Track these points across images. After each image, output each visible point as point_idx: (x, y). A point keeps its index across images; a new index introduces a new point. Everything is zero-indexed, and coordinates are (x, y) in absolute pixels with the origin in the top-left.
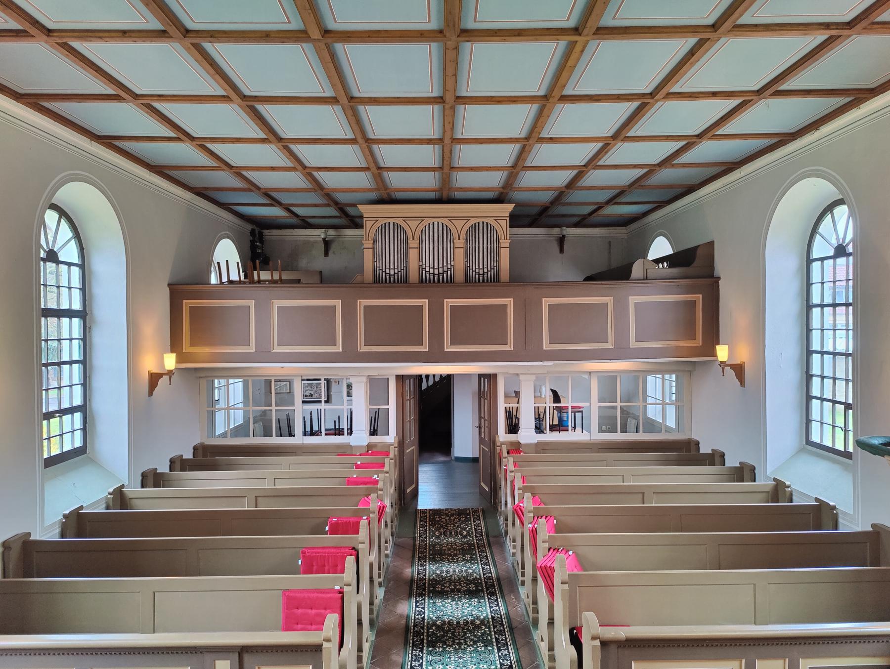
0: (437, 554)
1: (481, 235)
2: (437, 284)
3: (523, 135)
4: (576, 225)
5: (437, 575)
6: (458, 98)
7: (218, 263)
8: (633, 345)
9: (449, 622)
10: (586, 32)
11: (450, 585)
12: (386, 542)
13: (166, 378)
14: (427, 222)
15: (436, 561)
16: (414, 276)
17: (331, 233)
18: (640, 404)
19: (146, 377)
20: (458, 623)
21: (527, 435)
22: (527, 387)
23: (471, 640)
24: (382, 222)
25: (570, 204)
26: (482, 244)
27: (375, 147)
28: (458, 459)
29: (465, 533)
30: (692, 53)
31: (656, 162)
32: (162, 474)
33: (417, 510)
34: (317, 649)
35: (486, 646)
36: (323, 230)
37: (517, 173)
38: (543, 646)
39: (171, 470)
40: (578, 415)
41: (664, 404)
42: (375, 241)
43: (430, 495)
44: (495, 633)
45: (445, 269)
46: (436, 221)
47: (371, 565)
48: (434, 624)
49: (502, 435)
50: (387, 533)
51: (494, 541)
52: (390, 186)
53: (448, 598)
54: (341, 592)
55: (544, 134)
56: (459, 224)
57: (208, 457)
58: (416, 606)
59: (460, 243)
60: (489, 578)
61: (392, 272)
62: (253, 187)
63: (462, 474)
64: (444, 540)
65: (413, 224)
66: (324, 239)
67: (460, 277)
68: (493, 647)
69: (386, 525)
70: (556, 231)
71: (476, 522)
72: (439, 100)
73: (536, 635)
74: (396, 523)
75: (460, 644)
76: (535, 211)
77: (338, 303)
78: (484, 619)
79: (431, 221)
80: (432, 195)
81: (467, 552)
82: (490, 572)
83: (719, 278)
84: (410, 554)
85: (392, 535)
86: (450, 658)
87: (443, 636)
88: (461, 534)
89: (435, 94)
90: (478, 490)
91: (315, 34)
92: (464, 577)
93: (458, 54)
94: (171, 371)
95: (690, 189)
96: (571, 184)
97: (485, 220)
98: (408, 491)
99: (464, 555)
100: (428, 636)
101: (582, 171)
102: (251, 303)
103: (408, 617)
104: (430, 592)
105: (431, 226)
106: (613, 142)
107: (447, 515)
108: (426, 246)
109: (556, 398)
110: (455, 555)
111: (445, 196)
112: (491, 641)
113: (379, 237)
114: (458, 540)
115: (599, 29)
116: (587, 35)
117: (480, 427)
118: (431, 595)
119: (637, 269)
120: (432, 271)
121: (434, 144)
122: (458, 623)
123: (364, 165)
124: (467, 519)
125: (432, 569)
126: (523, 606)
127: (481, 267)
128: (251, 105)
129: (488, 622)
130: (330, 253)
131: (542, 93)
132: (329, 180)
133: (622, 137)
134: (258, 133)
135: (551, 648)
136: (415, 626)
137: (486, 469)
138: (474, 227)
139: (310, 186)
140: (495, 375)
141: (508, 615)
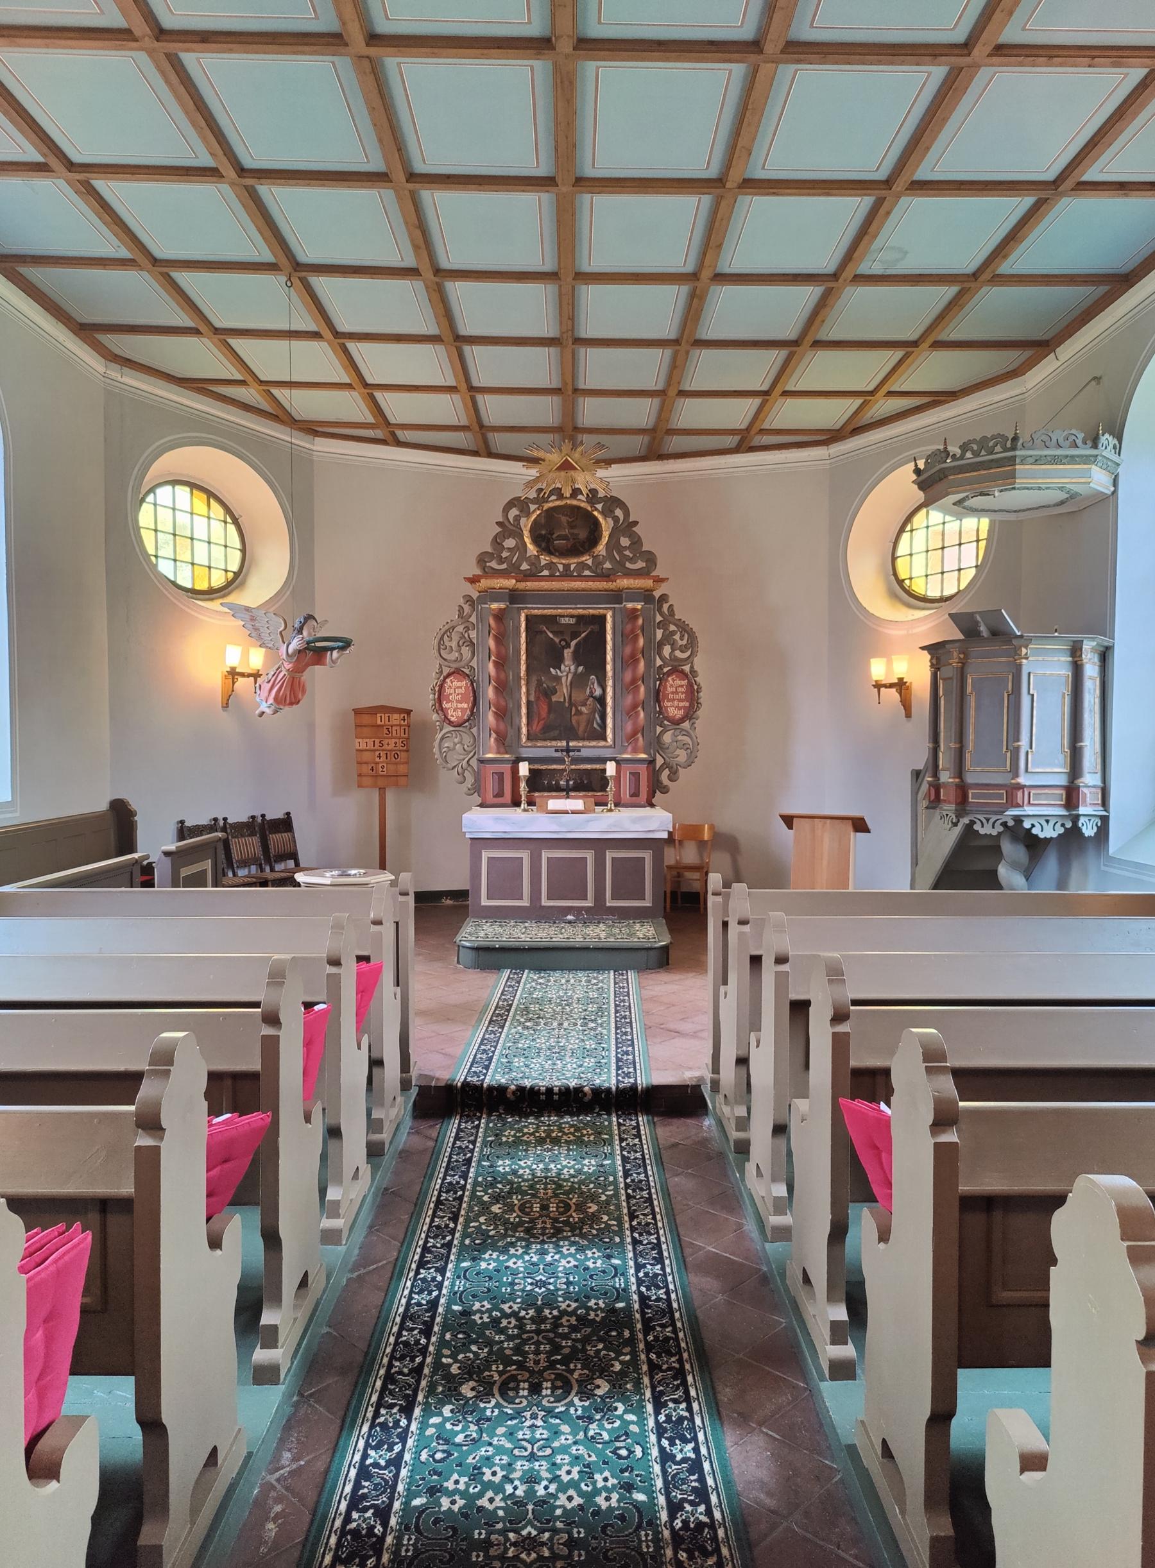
20: (535, 1389)
23: (502, 1331)
35: (466, 1313)
68: (448, 1309)
75: (539, 1319)
86: (568, 1283)
100: (632, 1342)
103: (716, 1410)
141: (347, 1424)
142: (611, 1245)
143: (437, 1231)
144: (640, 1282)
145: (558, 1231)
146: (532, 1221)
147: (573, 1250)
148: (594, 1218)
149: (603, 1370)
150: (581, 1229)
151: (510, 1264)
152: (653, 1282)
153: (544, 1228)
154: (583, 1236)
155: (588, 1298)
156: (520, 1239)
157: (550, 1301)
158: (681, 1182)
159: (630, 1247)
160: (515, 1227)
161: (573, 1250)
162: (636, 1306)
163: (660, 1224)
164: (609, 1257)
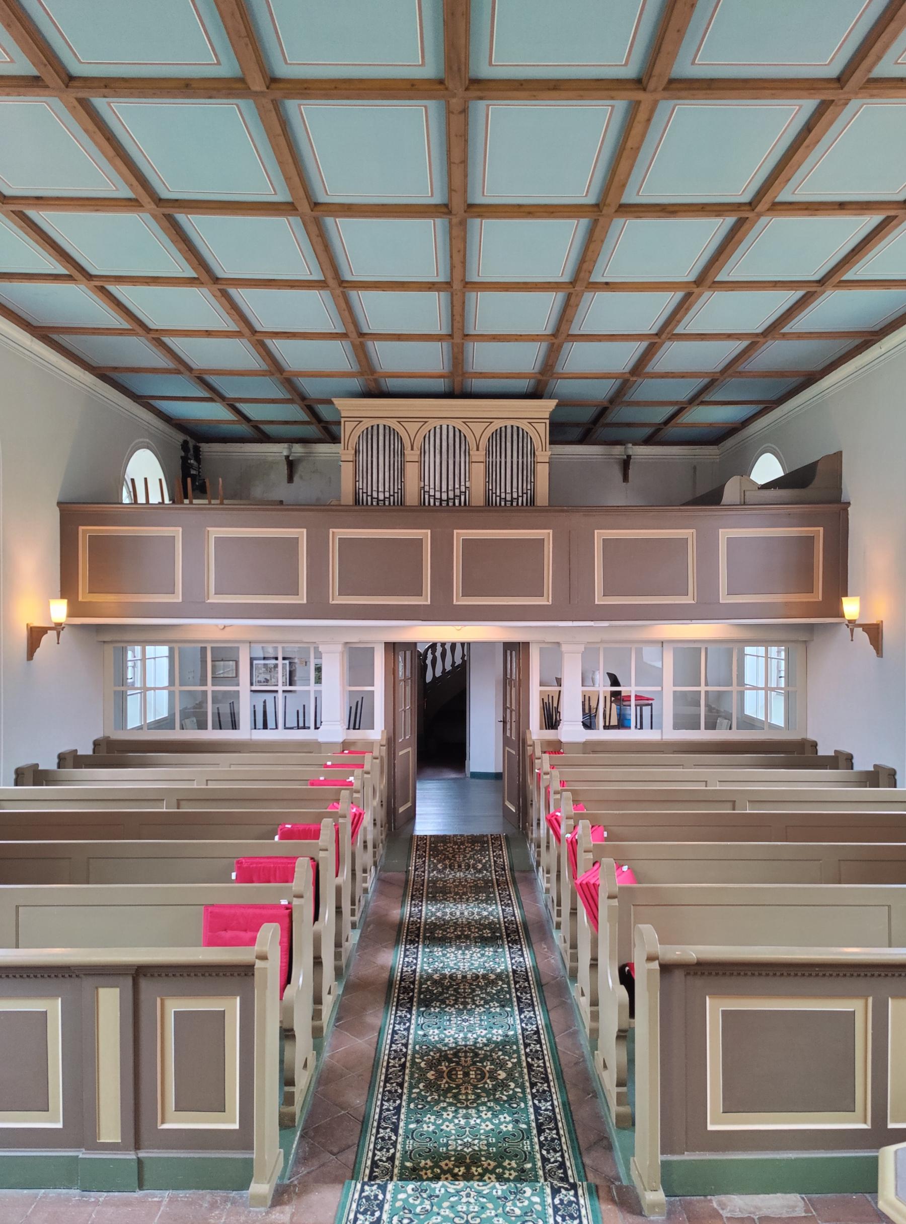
0: (439, 892)
1: (509, 445)
2: (446, 511)
3: (566, 278)
4: (648, 441)
5: (438, 918)
6: (470, 206)
7: (133, 480)
8: (724, 598)
9: (451, 977)
10: (652, 85)
11: (455, 930)
12: (365, 871)
13: (52, 634)
14: (432, 424)
15: (436, 900)
16: (412, 498)
17: (298, 449)
18: (734, 688)
19: (24, 634)
20: (464, 977)
21: (571, 730)
22: (571, 664)
23: (482, 999)
24: (367, 423)
25: (638, 404)
26: (511, 457)
27: (353, 294)
28: (475, 775)
29: (480, 866)
30: (808, 128)
31: (760, 331)
32: (46, 772)
33: (412, 837)
34: (246, 971)
36: (286, 445)
37: (560, 347)
38: (584, 1002)
39: (59, 767)
40: (646, 710)
41: (767, 689)
42: (357, 452)
43: (432, 816)
44: (517, 990)
45: (457, 492)
46: (444, 423)
47: (339, 890)
48: (430, 977)
49: (536, 732)
50: (366, 858)
51: (522, 875)
52: (378, 369)
53: (451, 946)
54: (289, 908)
55: (596, 277)
56: (478, 428)
57: (112, 753)
58: (405, 956)
59: (479, 455)
60: (511, 922)
61: (381, 497)
62: (182, 366)
63: (482, 795)
64: (450, 875)
65: (412, 427)
66: (287, 457)
67: (478, 497)
68: (512, 1007)
69: (365, 847)
70: (618, 450)
71: (497, 855)
72: (443, 210)
73: (574, 990)
74: (381, 850)
75: (465, 1004)
76: (587, 415)
77: (301, 534)
78: (502, 973)
79: (437, 423)
80: (440, 385)
81: (481, 890)
82: (514, 915)
83: (849, 503)
84: (401, 891)
85: (375, 864)
86: (450, 1020)
87: (441, 994)
88: (474, 868)
89: (437, 199)
90: (501, 814)
91: (257, 85)
92: (476, 921)
93: (466, 124)
94: (61, 624)
95: (810, 379)
96: (639, 368)
97: (516, 423)
98: (401, 810)
99: (477, 893)
100: (420, 993)
101: (654, 343)
102: (177, 532)
103: (392, 969)
104: (425, 938)
105: (438, 430)
106: (696, 290)
107: (455, 843)
108: (430, 459)
109: (615, 682)
110: (465, 894)
111: (457, 390)
112: (511, 999)
113: (363, 447)
114: (470, 875)
115: (671, 81)
116: (655, 90)
117: (504, 722)
118: (427, 942)
119: (731, 491)
120: (438, 495)
121: (438, 290)
122: (464, 977)
123: (340, 329)
124: (483, 849)
125: (430, 911)
126: (558, 958)
127: (509, 490)
128: (169, 213)
129: (507, 976)
130: (296, 478)
131: (591, 200)
132: (292, 355)
133: (708, 282)
134: (182, 268)
135: (594, 1003)
136: (402, 980)
137: (515, 783)
138: (499, 434)
139: (265, 367)
140: (527, 645)
141: (535, 968)
142: (421, 1044)
143: (537, 1055)
144: (409, 1020)
145: (456, 1055)
146: (474, 1063)
147: (447, 1040)
148: (431, 1065)
149: (435, 982)
150: (440, 1056)
151: (485, 1032)
152: (402, 1020)
153: (466, 1057)
154: (440, 1050)
155: (439, 1012)
156: (481, 1049)
157: (460, 1012)
158: (356, 1100)
159: (410, 1041)
160: (485, 1058)
161: (447, 1040)
162: (414, 1008)
163: (386, 1058)
164: (425, 1035)
